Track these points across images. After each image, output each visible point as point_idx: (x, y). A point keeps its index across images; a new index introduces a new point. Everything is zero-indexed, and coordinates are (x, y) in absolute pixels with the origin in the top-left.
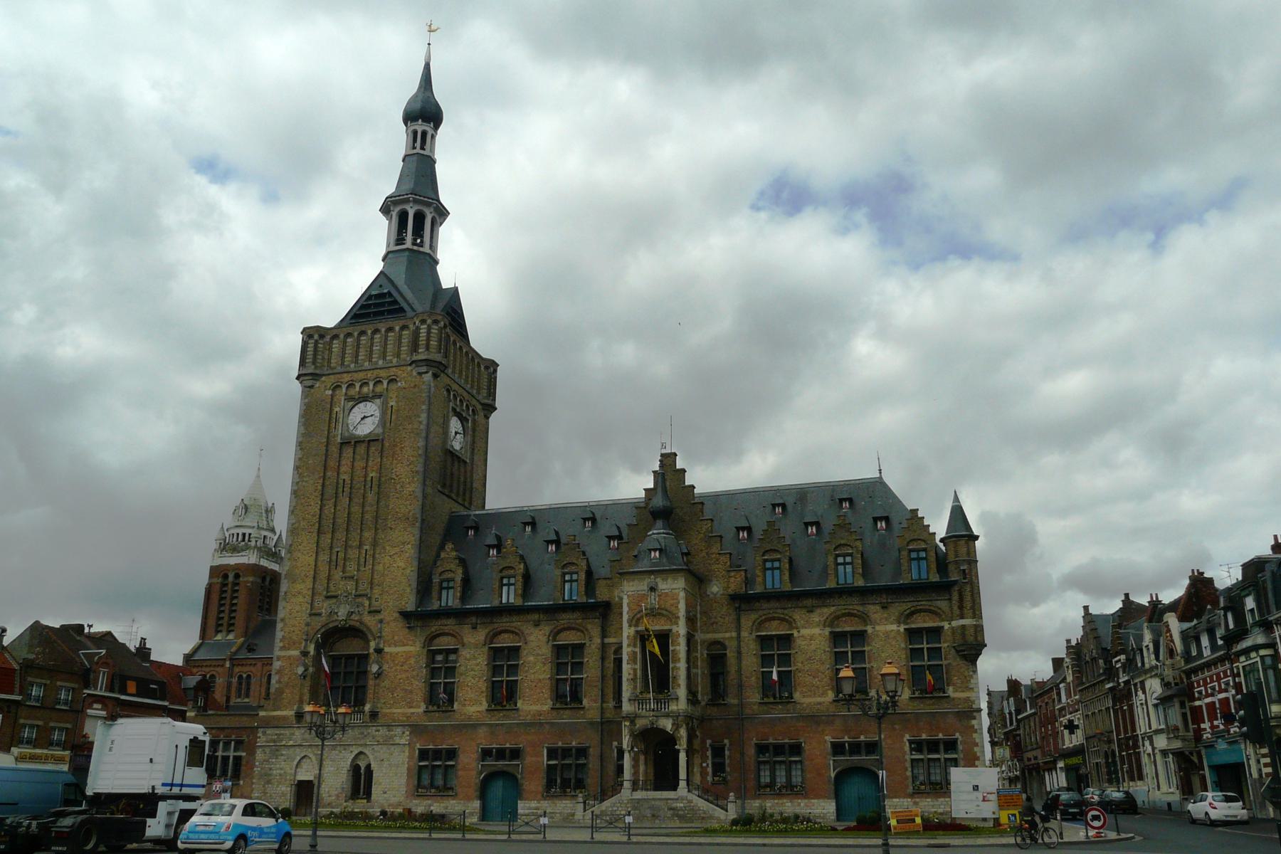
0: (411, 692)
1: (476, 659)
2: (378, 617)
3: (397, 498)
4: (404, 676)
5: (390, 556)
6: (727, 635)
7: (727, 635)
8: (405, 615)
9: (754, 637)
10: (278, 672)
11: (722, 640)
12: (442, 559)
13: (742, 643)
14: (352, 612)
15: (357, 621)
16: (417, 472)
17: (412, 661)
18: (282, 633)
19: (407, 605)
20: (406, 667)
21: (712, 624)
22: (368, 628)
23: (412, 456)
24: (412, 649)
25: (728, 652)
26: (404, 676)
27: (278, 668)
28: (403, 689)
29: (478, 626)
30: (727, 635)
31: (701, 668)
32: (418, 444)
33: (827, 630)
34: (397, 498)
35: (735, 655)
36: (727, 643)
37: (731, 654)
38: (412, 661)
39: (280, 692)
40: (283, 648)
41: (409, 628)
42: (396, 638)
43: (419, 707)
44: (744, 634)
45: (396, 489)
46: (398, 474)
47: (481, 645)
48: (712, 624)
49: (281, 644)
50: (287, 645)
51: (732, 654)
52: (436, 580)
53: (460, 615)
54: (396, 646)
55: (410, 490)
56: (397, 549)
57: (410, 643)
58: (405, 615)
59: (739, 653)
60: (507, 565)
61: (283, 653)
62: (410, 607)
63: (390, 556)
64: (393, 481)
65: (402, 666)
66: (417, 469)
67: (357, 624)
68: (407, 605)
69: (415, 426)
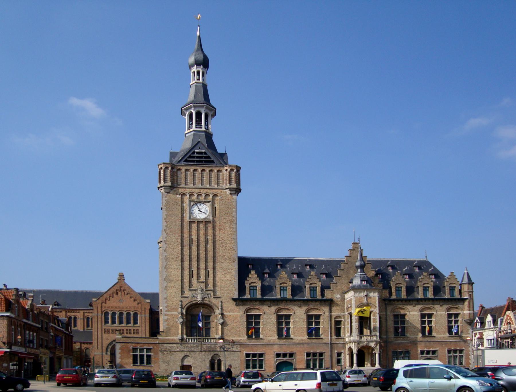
0: (239, 331)
1: (271, 319)
2: (220, 300)
5: (223, 274)
8: (234, 300)
12: (250, 278)
14: (205, 297)
15: (208, 301)
16: (233, 238)
17: (239, 319)
19: (234, 296)
20: (236, 321)
22: (214, 304)
23: (231, 231)
24: (238, 314)
26: (235, 324)
28: (235, 330)
32: (233, 226)
34: (224, 249)
41: (236, 305)
42: (229, 309)
43: (244, 337)
45: (223, 245)
46: (223, 238)
47: (272, 314)
52: (247, 286)
53: (262, 301)
54: (229, 312)
55: (231, 246)
56: (226, 272)
57: (237, 311)
58: (234, 300)
60: (283, 282)
62: (236, 296)
63: (223, 274)
64: (221, 241)
65: (234, 320)
66: (233, 237)
67: (208, 303)
68: (234, 296)
69: (231, 218)
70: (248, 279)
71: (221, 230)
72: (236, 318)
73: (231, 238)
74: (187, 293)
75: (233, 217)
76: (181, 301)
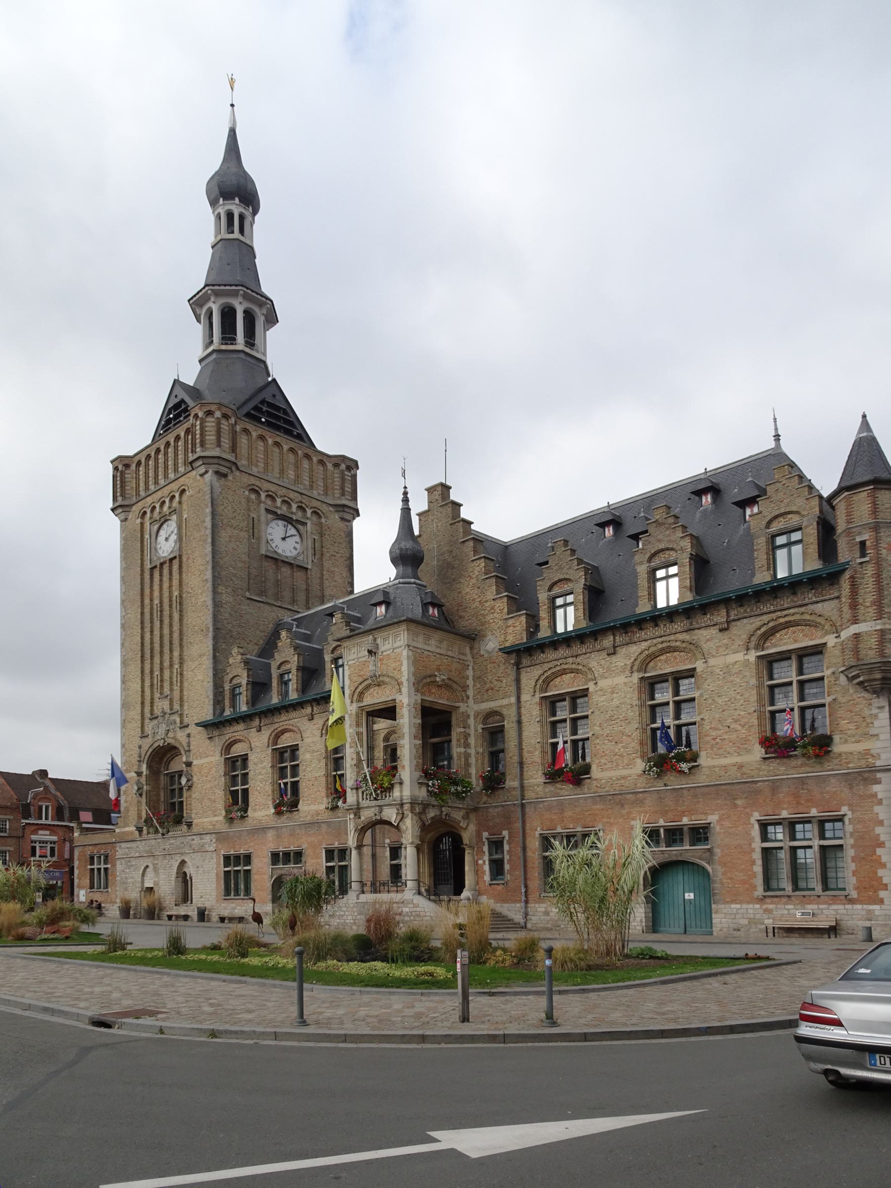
1: (262, 762)
6: (505, 703)
7: (505, 702)
9: (538, 700)
11: (498, 709)
13: (523, 709)
15: (172, 738)
21: (487, 690)
25: (505, 723)
29: (262, 728)
30: (505, 702)
31: (475, 747)
33: (636, 677)
35: (515, 725)
36: (505, 712)
37: (510, 726)
41: (209, 738)
42: (201, 750)
44: (525, 697)
48: (487, 690)
51: (511, 725)
54: (201, 758)
57: (212, 753)
58: (205, 725)
59: (519, 722)
74: (149, 726)
76: (140, 747)
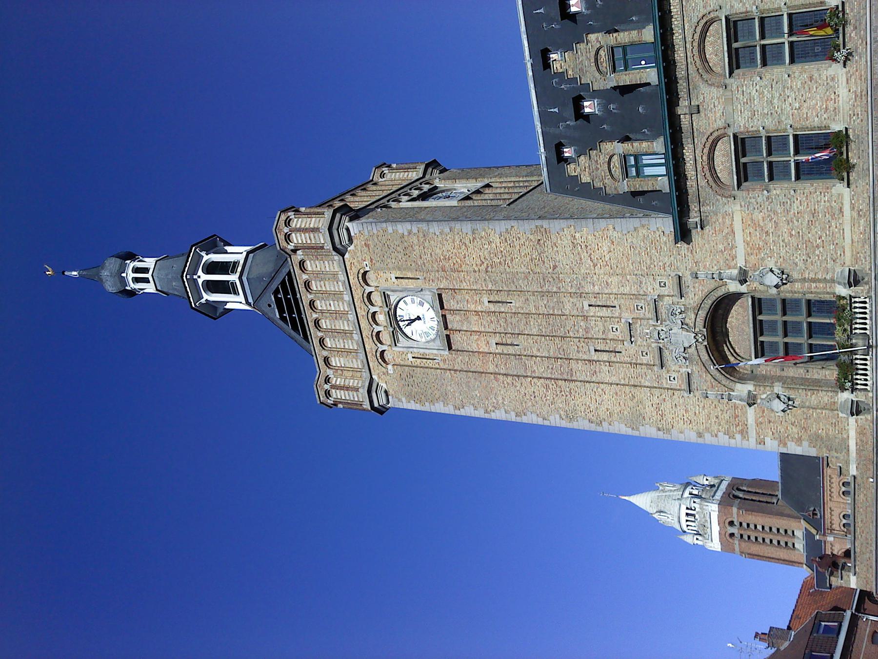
0: (814, 214)
3: (512, 260)
4: (785, 229)
5: (595, 266)
8: (683, 234)
10: (783, 442)
17: (758, 216)
18: (720, 434)
20: (770, 227)
24: (737, 218)
26: (785, 229)
27: (776, 443)
28: (809, 228)
34: (512, 260)
38: (758, 216)
39: (815, 439)
40: (744, 433)
42: (721, 247)
46: (479, 262)
49: (738, 436)
50: (739, 428)
55: (498, 240)
56: (584, 255)
57: (728, 222)
61: (752, 433)
63: (595, 266)
64: (489, 269)
66: (470, 233)
70: (598, 184)
71: (456, 266)
72: (755, 225)
73: (474, 238)
75: (410, 233)
